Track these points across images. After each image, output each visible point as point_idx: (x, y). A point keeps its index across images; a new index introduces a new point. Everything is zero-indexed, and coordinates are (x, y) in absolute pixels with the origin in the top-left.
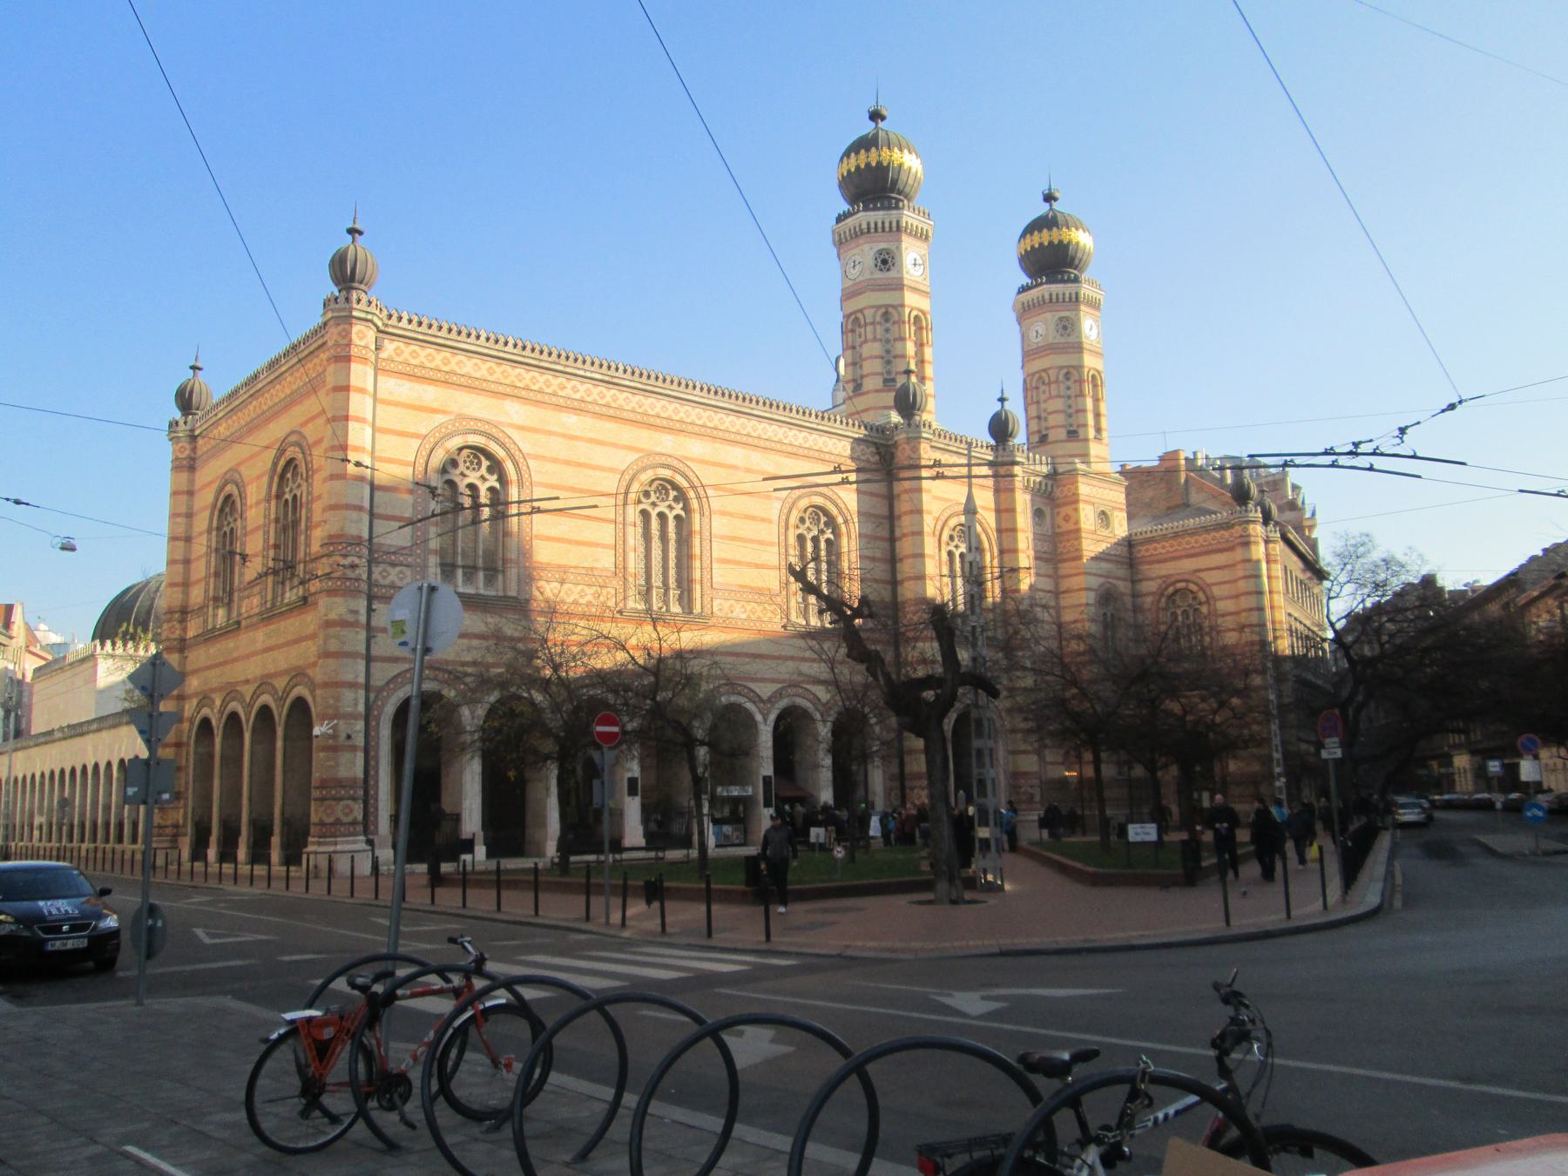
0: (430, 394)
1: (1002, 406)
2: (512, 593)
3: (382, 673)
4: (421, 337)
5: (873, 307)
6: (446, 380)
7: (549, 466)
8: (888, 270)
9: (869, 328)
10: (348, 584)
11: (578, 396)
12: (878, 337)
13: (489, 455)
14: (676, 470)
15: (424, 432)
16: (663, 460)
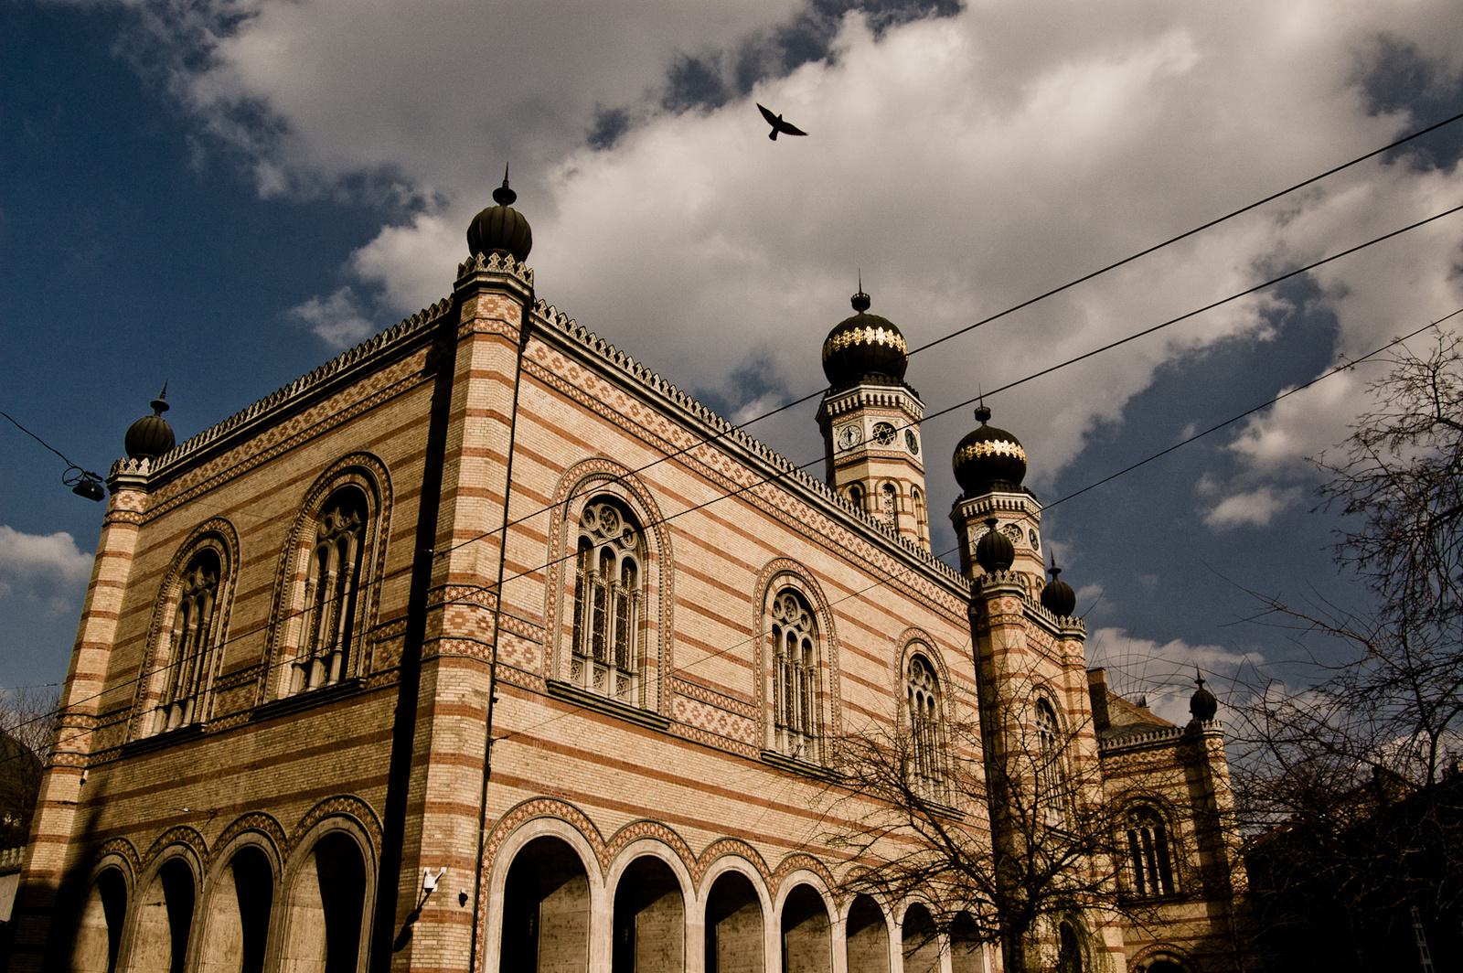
0: (573, 419)
1: (1055, 577)
2: (652, 707)
3: (502, 799)
4: (568, 343)
5: (874, 478)
6: (590, 407)
7: (690, 546)
8: (888, 443)
9: (873, 498)
10: (476, 649)
11: (716, 467)
12: (880, 508)
13: (630, 516)
14: (806, 583)
15: (562, 464)
16: (799, 570)
